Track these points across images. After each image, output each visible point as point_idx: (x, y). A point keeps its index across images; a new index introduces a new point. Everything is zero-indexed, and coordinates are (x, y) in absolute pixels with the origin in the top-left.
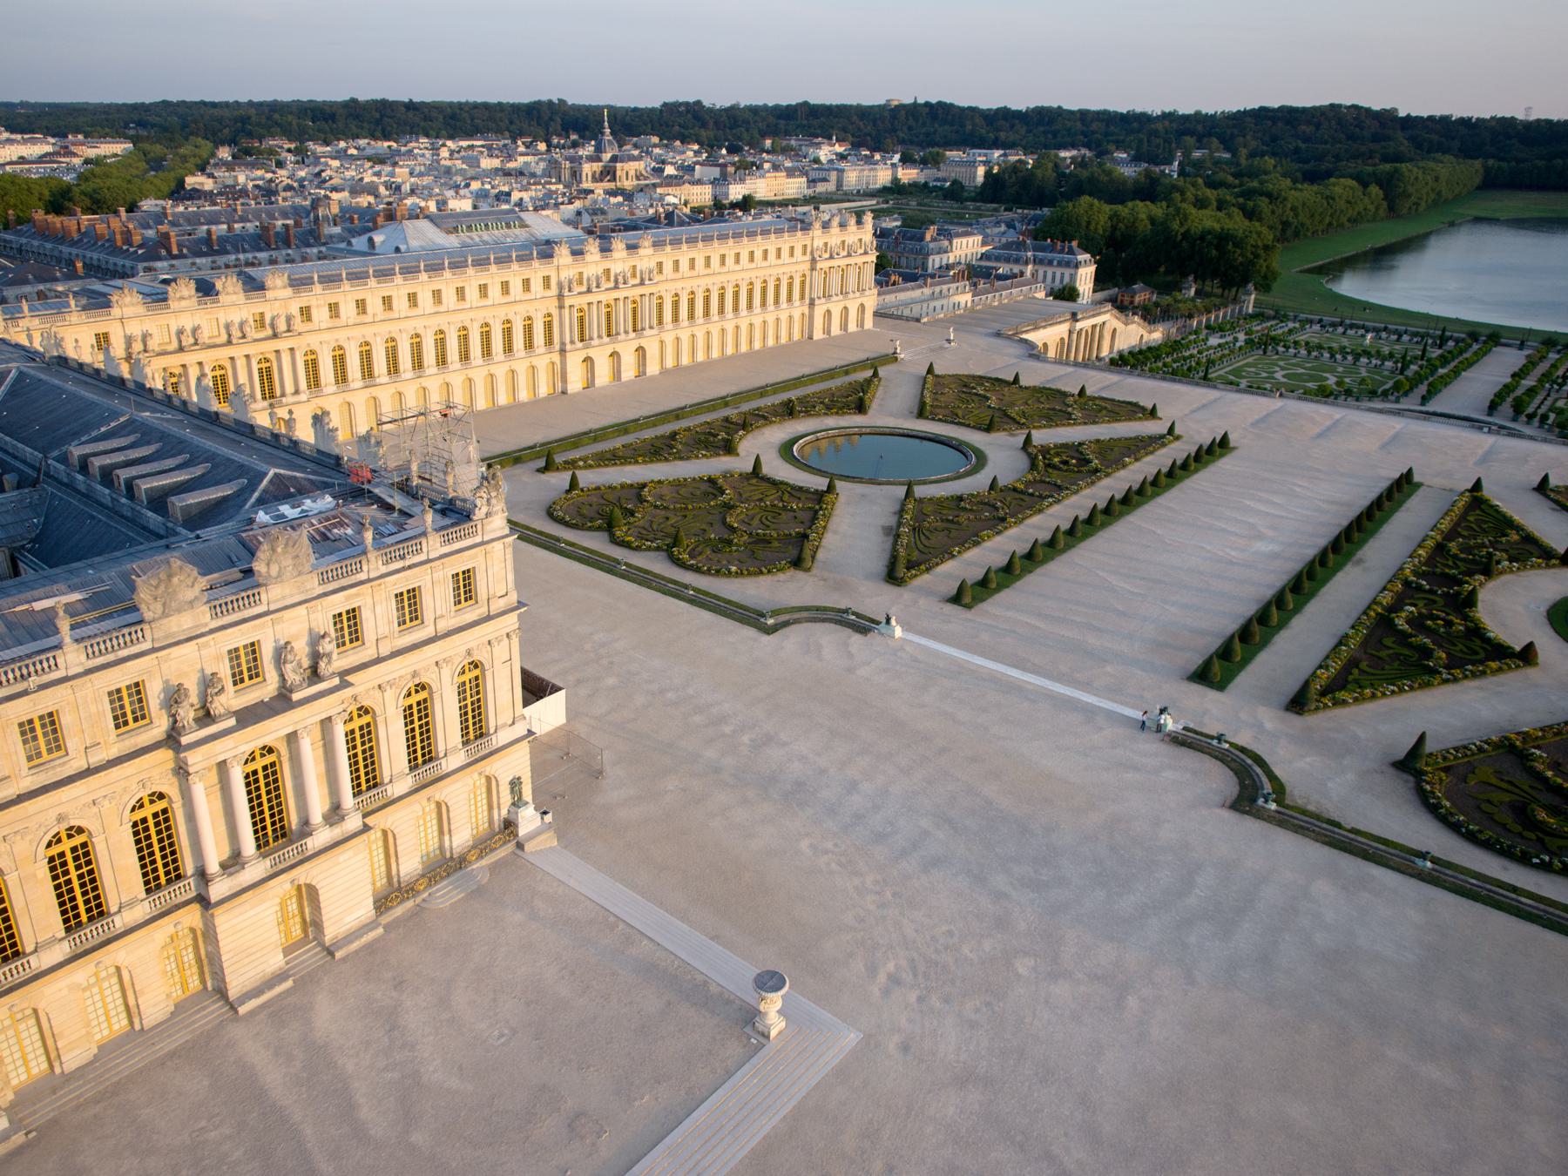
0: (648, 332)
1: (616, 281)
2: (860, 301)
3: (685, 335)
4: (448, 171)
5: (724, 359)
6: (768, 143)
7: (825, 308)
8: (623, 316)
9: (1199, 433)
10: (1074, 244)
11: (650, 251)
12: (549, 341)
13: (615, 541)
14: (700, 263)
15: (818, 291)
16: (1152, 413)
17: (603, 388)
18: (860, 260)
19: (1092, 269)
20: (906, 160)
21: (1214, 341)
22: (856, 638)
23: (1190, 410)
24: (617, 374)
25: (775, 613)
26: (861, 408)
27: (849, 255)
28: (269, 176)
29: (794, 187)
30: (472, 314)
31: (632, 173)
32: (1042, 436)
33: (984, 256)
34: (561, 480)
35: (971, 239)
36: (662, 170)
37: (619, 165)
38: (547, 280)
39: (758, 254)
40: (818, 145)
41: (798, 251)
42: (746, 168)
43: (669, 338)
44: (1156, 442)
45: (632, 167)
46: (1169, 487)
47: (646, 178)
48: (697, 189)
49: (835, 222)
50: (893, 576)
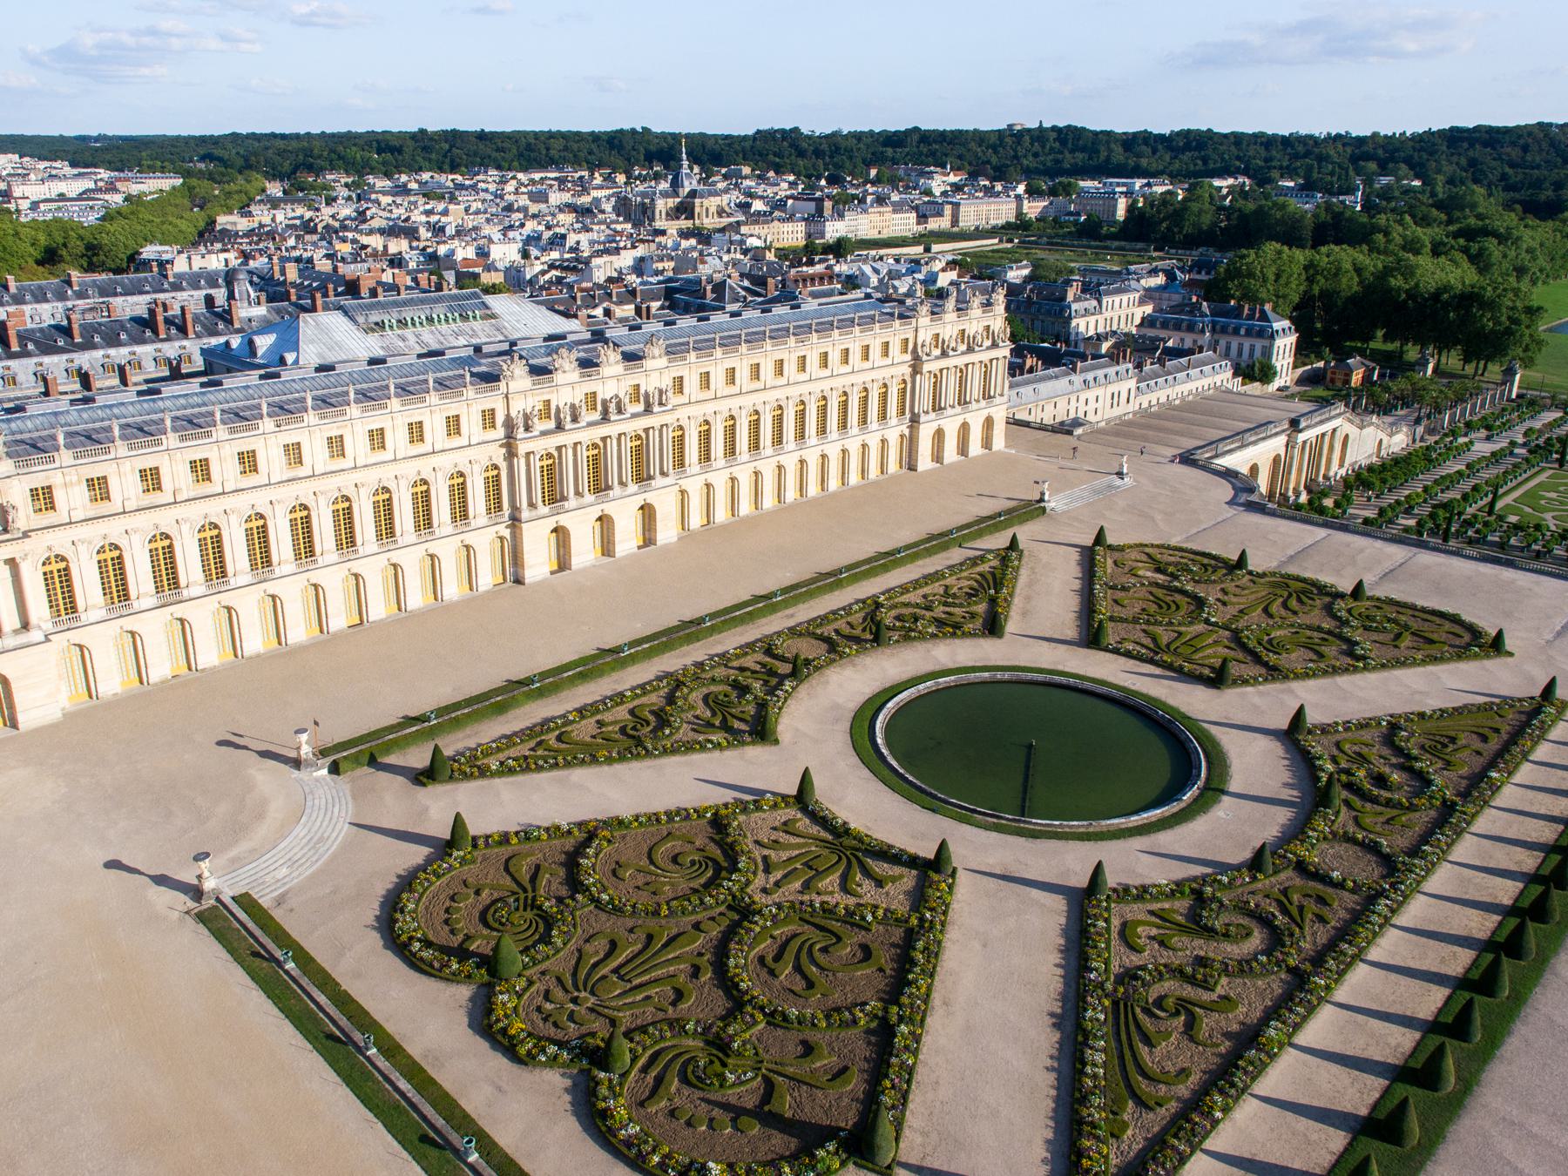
0: (659, 481)
1: (605, 412)
2: (985, 413)
3: (720, 480)
4: (509, 208)
7: (935, 426)
8: (618, 463)
11: (664, 361)
12: (495, 505)
14: (743, 374)
15: (924, 401)
17: (584, 570)
27: (970, 350)
28: (308, 215)
30: (357, 476)
38: (489, 418)
39: (835, 357)
41: (895, 349)
43: (694, 486)
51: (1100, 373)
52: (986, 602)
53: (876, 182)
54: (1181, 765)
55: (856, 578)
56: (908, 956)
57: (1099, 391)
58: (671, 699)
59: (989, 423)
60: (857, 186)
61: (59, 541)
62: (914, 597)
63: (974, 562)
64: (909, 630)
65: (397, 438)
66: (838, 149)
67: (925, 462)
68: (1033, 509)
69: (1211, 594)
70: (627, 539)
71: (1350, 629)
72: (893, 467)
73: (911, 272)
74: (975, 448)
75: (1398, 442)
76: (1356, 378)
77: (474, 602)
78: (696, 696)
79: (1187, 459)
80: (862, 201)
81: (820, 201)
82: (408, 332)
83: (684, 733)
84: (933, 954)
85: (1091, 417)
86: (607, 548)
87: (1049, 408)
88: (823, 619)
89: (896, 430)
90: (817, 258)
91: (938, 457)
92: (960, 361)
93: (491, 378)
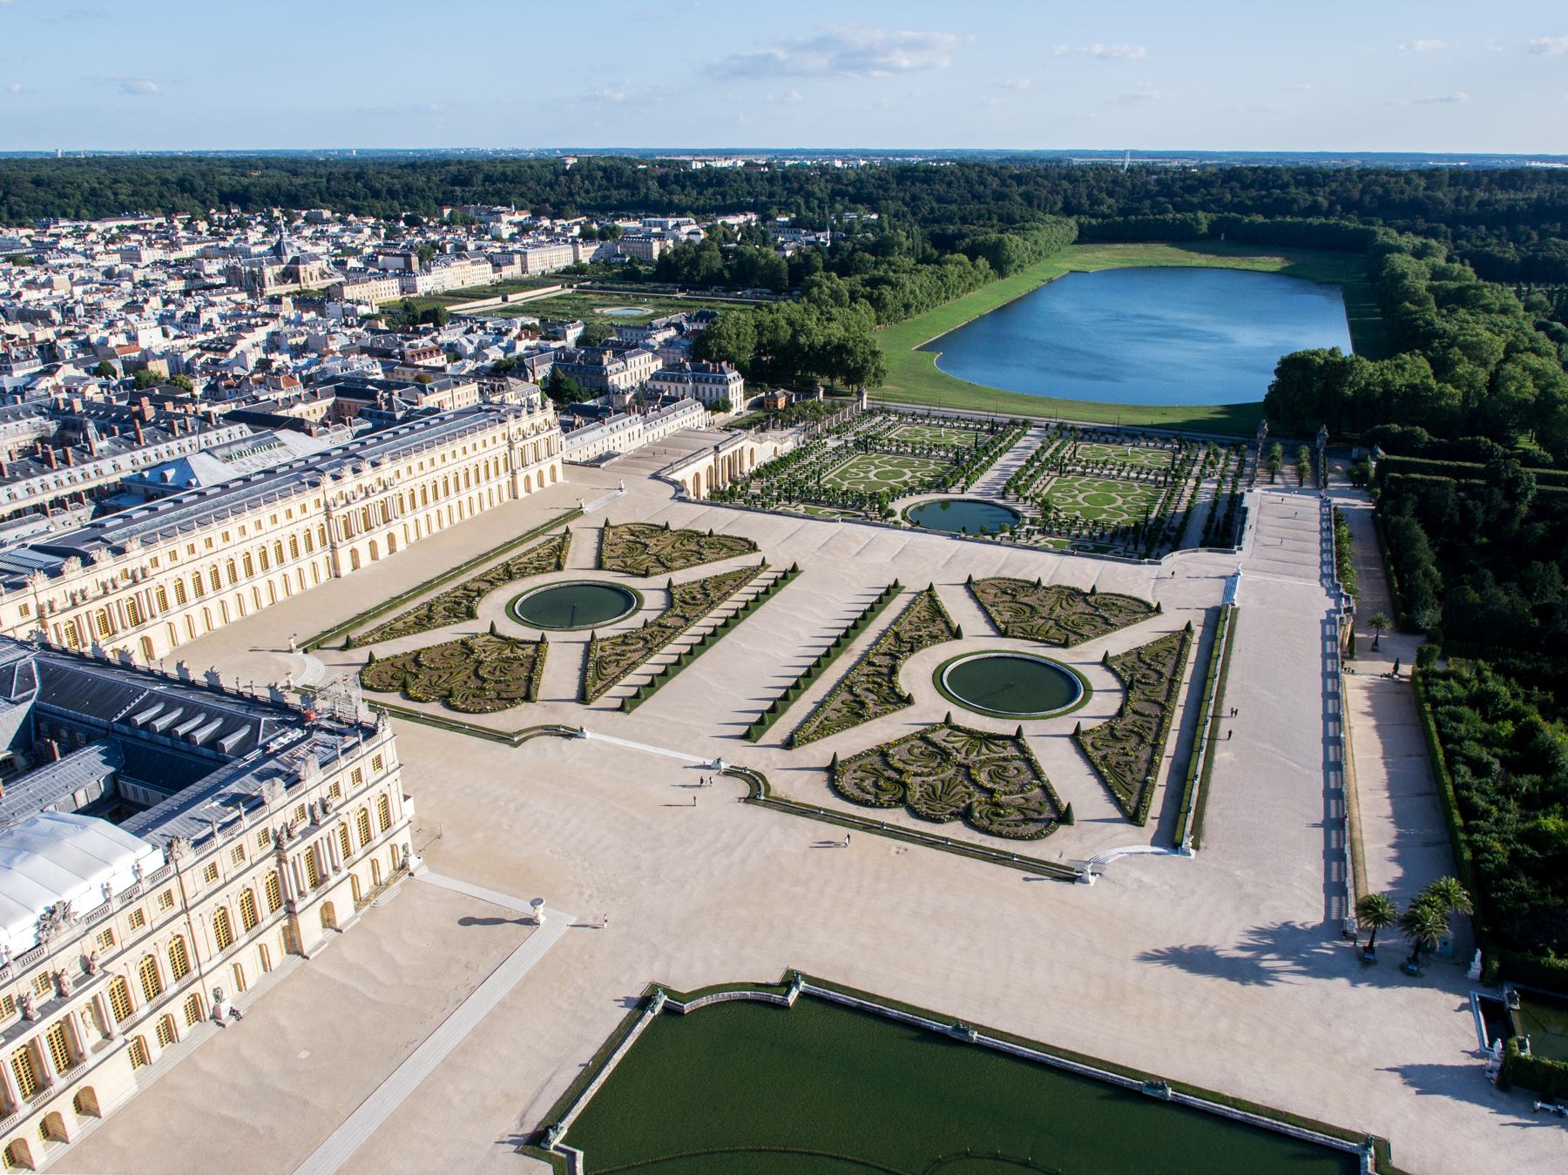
0: (395, 521)
5: (454, 527)
6: (447, 212)
9: (780, 564)
10: (724, 364)
13: (407, 696)
15: (517, 462)
16: (753, 547)
18: (546, 435)
19: (741, 382)
20: (587, 236)
21: (832, 443)
22: (566, 741)
23: (780, 536)
24: (374, 556)
25: (519, 733)
26: (559, 567)
29: (479, 274)
31: (316, 273)
32: (681, 577)
33: (655, 377)
34: (360, 655)
35: (642, 358)
36: (345, 263)
37: (301, 267)
40: (497, 216)
41: (499, 439)
42: (430, 255)
43: (410, 522)
44: (753, 572)
45: (314, 267)
46: (755, 609)
47: (330, 276)
48: (384, 284)
49: (524, 411)
50: (583, 698)
51: (620, 423)
52: (556, 557)
53: (451, 222)
54: (627, 600)
55: (497, 555)
56: (534, 664)
57: (621, 434)
58: (430, 610)
59: (553, 468)
60: (434, 229)
61: (160, 579)
62: (524, 560)
63: (550, 541)
64: (523, 573)
65: (282, 518)
66: (410, 189)
67: (522, 494)
68: (577, 513)
69: (651, 542)
70: (383, 551)
71: (699, 545)
72: (506, 498)
73: (496, 342)
74: (548, 482)
75: (788, 446)
76: (781, 403)
77: (320, 589)
78: (440, 608)
79: (655, 477)
80: (443, 249)
81: (407, 257)
82: (244, 459)
83: (440, 621)
84: (543, 662)
85: (618, 450)
86: (374, 556)
87: (591, 448)
88: (486, 574)
89: (505, 478)
90: (421, 327)
91: (528, 490)
92: (534, 440)
93: (314, 484)
